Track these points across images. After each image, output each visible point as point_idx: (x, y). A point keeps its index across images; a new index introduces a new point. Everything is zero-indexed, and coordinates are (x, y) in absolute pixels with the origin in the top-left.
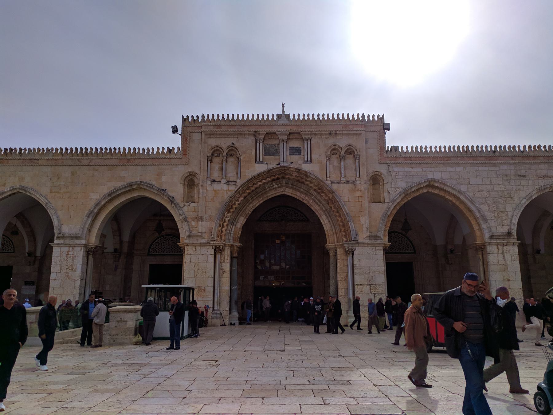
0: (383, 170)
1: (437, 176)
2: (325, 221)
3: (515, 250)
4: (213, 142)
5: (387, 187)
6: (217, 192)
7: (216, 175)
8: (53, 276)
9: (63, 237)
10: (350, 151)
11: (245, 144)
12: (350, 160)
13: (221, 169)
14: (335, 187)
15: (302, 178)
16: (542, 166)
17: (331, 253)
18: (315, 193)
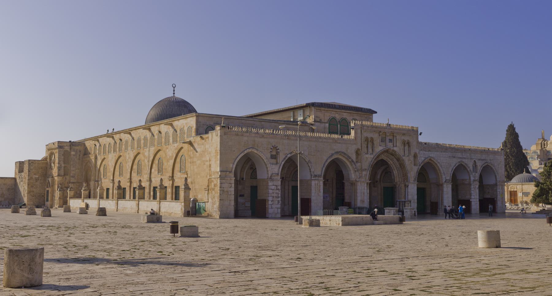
0: (417, 151)
1: (432, 155)
2: (395, 172)
3: (450, 186)
4: (365, 135)
5: (418, 159)
6: (368, 159)
7: (366, 150)
8: (313, 194)
9: (316, 176)
10: (408, 143)
11: (375, 136)
12: (407, 147)
13: (367, 147)
14: (404, 158)
15: (394, 154)
16: (459, 154)
17: (397, 186)
18: (395, 160)
